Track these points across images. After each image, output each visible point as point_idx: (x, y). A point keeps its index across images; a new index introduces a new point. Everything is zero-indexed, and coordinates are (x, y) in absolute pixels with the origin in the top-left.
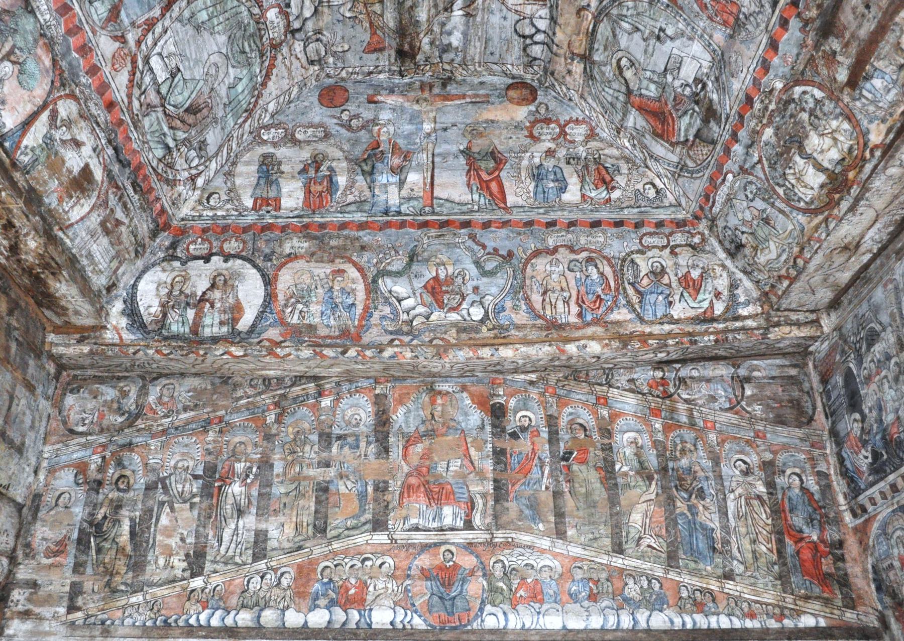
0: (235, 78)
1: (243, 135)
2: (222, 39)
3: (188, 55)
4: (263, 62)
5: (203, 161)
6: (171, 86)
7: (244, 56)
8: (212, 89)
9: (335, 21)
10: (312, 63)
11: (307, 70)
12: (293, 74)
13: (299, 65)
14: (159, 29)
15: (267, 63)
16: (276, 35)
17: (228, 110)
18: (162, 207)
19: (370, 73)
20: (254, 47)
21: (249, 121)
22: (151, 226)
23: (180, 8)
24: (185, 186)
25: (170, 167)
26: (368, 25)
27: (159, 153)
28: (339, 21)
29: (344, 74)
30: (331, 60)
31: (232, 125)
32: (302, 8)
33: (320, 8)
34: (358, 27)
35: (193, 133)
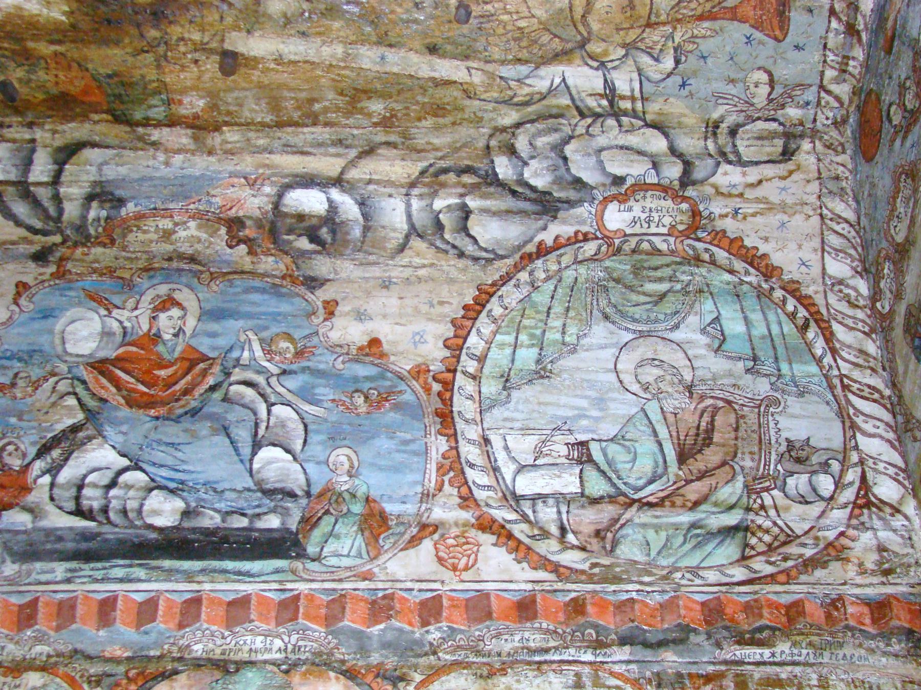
0: (703, 331)
1: (862, 352)
2: (600, 332)
3: (570, 413)
4: (713, 262)
5: (835, 466)
6: (603, 473)
7: (670, 297)
8: (690, 388)
9: (685, 92)
10: (787, 154)
11: (799, 168)
12: (790, 201)
13: (777, 183)
14: (471, 453)
15: (721, 255)
16: (667, 220)
17: (768, 367)
18: (867, 602)
19: (851, 30)
20: (667, 272)
21: (836, 327)
22: (897, 647)
23: (471, 397)
24: (863, 527)
25: (785, 543)
26: (706, 24)
27: (729, 551)
28: (683, 85)
29: (843, 90)
30: (793, 113)
31: (814, 369)
32: (640, 153)
33: (649, 117)
34: (706, 46)
35: (748, 463)
